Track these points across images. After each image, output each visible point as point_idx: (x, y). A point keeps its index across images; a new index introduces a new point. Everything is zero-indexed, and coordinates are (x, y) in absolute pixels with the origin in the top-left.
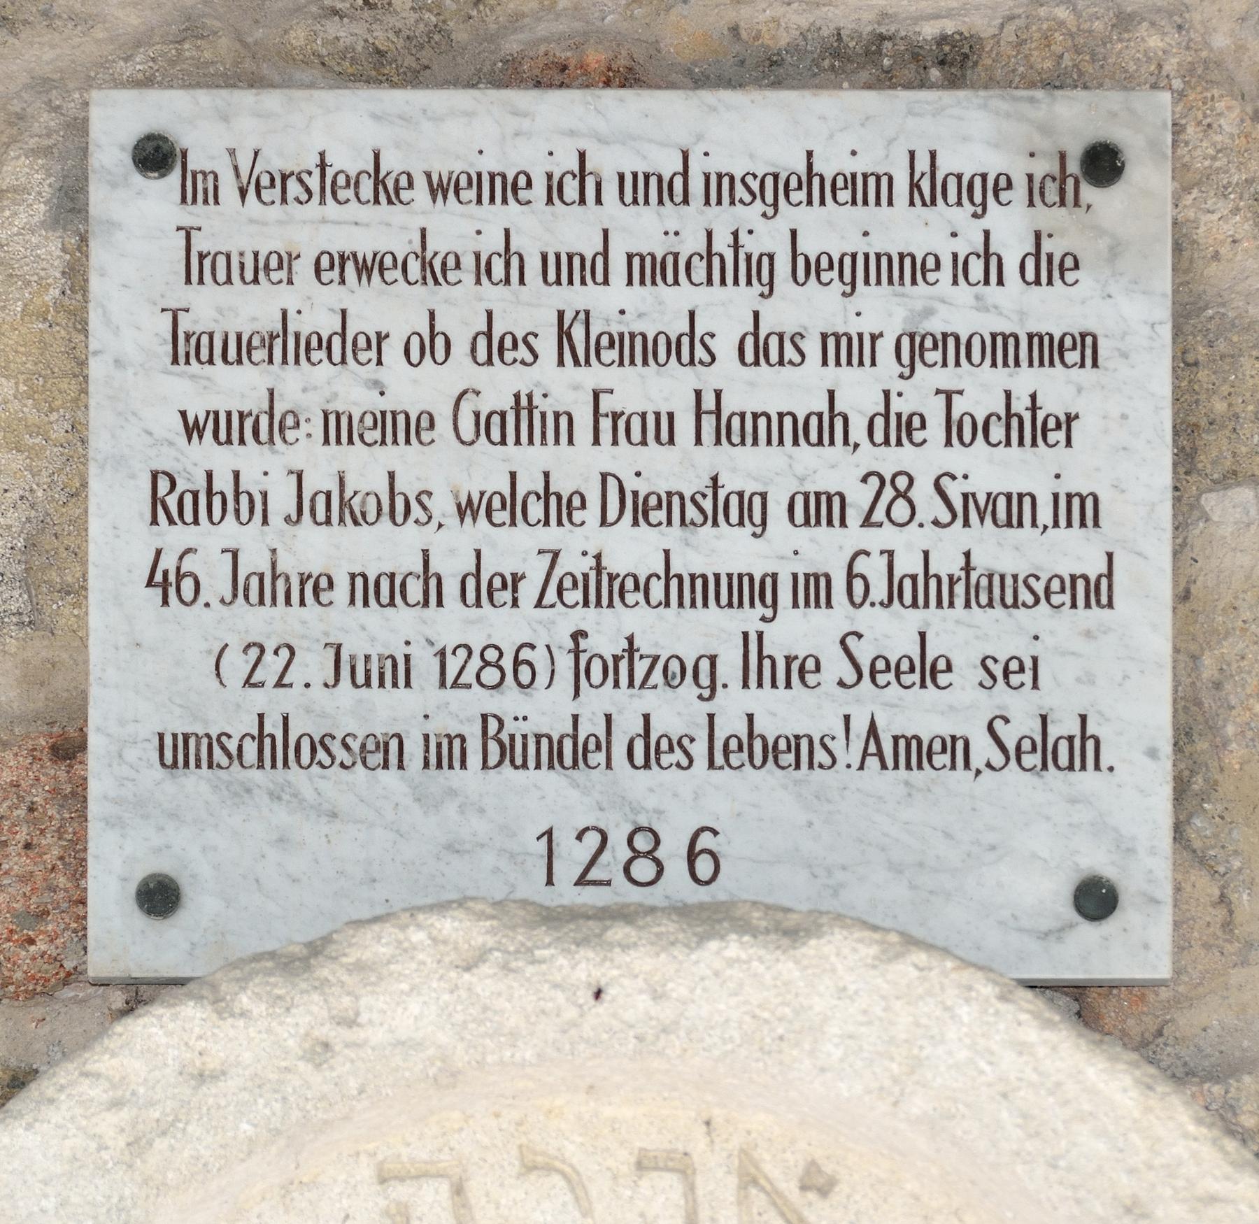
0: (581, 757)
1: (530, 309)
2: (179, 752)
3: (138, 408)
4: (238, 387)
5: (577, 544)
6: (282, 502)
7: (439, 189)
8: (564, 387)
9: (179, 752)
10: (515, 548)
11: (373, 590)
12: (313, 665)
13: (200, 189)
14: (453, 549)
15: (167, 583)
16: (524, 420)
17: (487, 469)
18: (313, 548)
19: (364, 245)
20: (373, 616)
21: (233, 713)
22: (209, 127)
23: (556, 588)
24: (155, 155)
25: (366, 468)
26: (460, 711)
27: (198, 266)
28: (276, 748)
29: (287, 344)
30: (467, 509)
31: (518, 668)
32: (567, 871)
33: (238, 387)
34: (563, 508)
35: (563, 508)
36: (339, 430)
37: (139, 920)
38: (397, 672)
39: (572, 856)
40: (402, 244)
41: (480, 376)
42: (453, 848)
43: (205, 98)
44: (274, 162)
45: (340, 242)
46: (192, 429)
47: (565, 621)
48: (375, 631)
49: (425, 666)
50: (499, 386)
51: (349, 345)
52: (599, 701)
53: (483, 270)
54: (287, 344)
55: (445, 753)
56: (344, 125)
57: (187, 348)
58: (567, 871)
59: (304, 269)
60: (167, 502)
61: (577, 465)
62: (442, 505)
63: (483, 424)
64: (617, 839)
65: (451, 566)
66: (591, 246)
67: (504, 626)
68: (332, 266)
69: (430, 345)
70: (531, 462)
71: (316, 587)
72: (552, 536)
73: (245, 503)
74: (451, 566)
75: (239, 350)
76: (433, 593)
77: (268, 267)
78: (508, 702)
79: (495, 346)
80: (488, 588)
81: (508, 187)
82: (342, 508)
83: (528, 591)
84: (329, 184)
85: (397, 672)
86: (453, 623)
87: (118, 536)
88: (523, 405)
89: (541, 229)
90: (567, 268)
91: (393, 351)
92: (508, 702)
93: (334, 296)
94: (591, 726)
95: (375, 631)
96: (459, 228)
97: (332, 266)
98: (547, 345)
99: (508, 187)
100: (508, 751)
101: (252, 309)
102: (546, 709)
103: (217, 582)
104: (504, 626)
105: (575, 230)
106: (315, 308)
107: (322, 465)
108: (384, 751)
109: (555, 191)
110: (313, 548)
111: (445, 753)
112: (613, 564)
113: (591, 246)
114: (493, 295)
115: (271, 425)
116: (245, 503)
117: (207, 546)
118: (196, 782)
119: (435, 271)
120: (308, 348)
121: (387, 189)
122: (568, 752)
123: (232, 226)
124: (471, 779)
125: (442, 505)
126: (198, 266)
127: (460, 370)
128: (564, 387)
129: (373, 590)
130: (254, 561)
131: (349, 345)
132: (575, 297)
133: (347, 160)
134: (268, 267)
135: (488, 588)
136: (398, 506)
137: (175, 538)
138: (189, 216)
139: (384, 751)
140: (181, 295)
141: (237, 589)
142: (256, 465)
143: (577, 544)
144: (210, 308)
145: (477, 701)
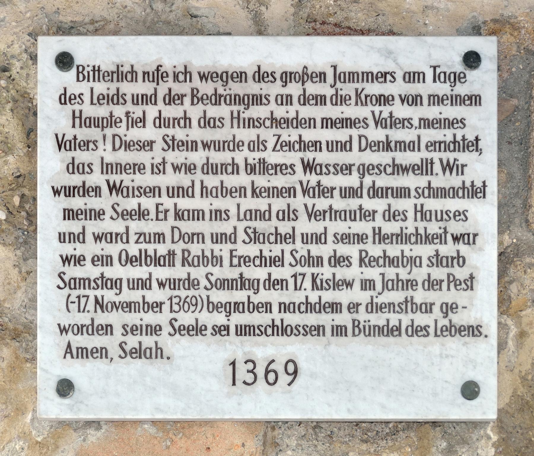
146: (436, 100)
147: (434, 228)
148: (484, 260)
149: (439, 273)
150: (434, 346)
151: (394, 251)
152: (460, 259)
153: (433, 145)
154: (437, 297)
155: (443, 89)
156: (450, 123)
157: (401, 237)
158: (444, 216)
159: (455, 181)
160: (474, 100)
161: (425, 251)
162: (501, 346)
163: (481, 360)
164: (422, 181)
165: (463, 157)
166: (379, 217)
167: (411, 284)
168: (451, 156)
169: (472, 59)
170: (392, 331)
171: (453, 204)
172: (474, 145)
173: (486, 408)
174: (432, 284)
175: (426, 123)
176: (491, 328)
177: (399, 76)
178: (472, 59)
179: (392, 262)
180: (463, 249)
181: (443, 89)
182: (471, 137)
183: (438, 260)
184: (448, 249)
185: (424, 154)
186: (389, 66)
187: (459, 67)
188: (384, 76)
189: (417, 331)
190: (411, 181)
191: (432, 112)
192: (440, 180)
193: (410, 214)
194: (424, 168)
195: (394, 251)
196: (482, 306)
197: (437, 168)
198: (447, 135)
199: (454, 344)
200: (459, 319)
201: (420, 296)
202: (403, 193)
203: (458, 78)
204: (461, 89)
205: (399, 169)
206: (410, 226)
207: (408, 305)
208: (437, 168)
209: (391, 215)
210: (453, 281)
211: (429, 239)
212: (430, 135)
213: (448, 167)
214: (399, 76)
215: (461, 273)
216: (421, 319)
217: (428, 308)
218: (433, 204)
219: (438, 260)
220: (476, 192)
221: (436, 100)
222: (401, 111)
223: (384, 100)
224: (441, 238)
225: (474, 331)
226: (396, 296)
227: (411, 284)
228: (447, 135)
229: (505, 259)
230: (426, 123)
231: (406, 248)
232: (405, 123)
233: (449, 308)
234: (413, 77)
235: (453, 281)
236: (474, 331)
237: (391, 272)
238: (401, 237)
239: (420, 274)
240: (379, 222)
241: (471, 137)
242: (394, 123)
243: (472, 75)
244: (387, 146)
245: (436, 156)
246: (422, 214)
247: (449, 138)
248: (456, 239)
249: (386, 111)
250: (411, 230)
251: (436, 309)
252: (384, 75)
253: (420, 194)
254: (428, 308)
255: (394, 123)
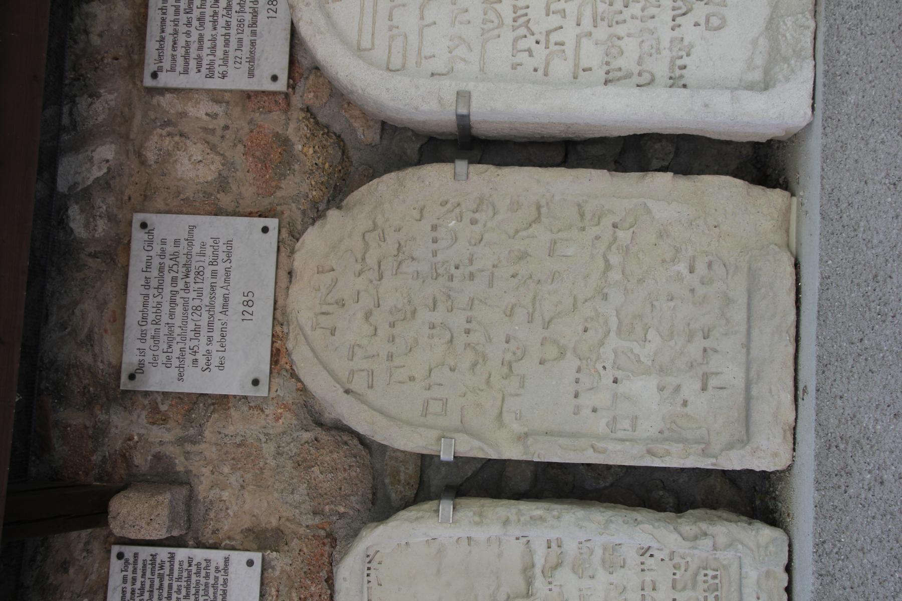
0: (256, 12)
1: (183, 18)
2: (251, 74)
3: (195, 80)
4: (193, 64)
5: (221, 12)
6: (212, 57)
7: (163, 32)
8: (196, 13)
9: (251, 74)
10: (222, 21)
11: (227, 43)
12: (238, 53)
13: (160, 69)
14: (221, 31)
15: (224, 76)
16: (201, 20)
17: (209, 25)
18: (220, 53)
19: (171, 43)
20: (231, 44)
21: (246, 66)
22: (150, 66)
23: (228, 15)
24: (154, 75)
25: (207, 44)
26: (247, 31)
27: (173, 70)
28: (251, 60)
29: (186, 58)
30: (215, 29)
31: (241, 22)
32: (274, 15)
33: (193, 64)
34: (216, 13)
35: (216, 13)
36: (200, 48)
37: (278, 82)
38: (240, 41)
39: (272, 14)
40: (171, 38)
41: (193, 26)
42: (269, 32)
43: (146, 68)
44: (157, 57)
45: (170, 48)
46: (199, 71)
47: (234, 14)
48: (233, 43)
49: (240, 36)
50: (195, 23)
51: (187, 45)
52: (247, 9)
53: (176, 25)
54: (186, 58)
55: (254, 33)
56: (152, 46)
57: (186, 71)
58: (274, 15)
59: (174, 53)
60: (210, 76)
61: (209, 11)
62: (214, 32)
63: (201, 26)
64: (269, 7)
65: (224, 31)
66: (174, 8)
67: (234, 23)
68: (174, 48)
69: (188, 34)
70: (208, 18)
71: (226, 52)
72: (220, 16)
73: (211, 64)
74: (224, 31)
75: (187, 63)
76: (228, 34)
77: (174, 58)
78: (246, 23)
79: (189, 24)
80: (228, 25)
81: (163, 20)
82: (213, 48)
83: (228, 19)
84: (161, 48)
85: (240, 41)
86: (233, 31)
87: (215, 84)
88: (199, 19)
89: (170, 16)
90: (177, 12)
91: (188, 40)
92: (246, 23)
93: (179, 49)
94: (251, 10)
95: (233, 43)
96: (169, 29)
97: (174, 48)
98: (189, 15)
99: (163, 20)
100: (254, 24)
101: (180, 61)
102: (248, 17)
103: (224, 68)
104: (234, 23)
105: (171, 11)
106: (181, 51)
107: (207, 51)
108: (253, 43)
109: (164, 14)
110: (220, 53)
111: (254, 33)
112: (225, 6)
113: (174, 8)
114: (181, 24)
115: (199, 59)
116: (211, 64)
117: (218, 69)
118: (256, 72)
119: (176, 33)
120: (187, 52)
121: (162, 39)
122: (255, 14)
123: (167, 63)
124: (258, 29)
125: (214, 32)
126: (173, 70)
127: (193, 29)
128: (196, 13)
129: (227, 43)
130: (221, 62)
131: (187, 45)
132: (182, 11)
133: (157, 46)
134: (174, 58)
135: (228, 25)
136: (214, 40)
137: (216, 74)
138: (165, 71)
139: (253, 43)
140: (177, 72)
141: (226, 65)
142: (205, 61)
143: (221, 12)
144: (180, 67)
145: (246, 28)
146: (135, 571)
147: (185, 574)
148: (200, 554)
149: (203, 573)
150: (232, 576)
151: (193, 591)
152: (199, 564)
153: (153, 573)
154: (213, 574)
155: (131, 568)
156: (144, 566)
157: (188, 588)
158: (181, 570)
159: (167, 565)
160: (136, 555)
161: (194, 578)
162: (233, 548)
163: (239, 558)
164: (166, 578)
165: (158, 561)
166: (179, 596)
167: (206, 584)
168: (157, 566)
169: (120, 556)
170: (225, 593)
171: (176, 566)
172: (154, 556)
173: (257, 557)
174: (207, 576)
175: (144, 575)
176: (226, 553)
177: (124, 585)
178: (120, 556)
179: (197, 592)
180: (194, 563)
181: (131, 568)
182: (151, 558)
183: (198, 573)
184: (194, 569)
185: (156, 577)
186: (120, 589)
187: (123, 561)
188: (124, 592)
189: (225, 582)
190: (166, 583)
191: (139, 572)
192: (167, 571)
193: (179, 583)
194: (161, 577)
195: (193, 591)
196: (217, 556)
197: (161, 572)
198: (149, 567)
199: (231, 569)
200: (221, 566)
201: (211, 581)
202: (170, 586)
203: (127, 561)
204: (131, 560)
205: (161, 587)
206: (184, 584)
207: (215, 586)
208: (161, 572)
209: (179, 591)
210: (207, 568)
211: (189, 577)
212: (148, 574)
213: (162, 568)
214: (124, 585)
215: (204, 564)
216: (221, 581)
217: (216, 578)
218: (176, 574)
219: (198, 573)
220: (172, 556)
221: (135, 571)
222: (138, 585)
223: (133, 591)
224: (189, 572)
225: (227, 560)
226: (211, 591)
227: (206, 584)
228: (149, 567)
229: (200, 545)
230: (144, 575)
231: (192, 586)
232: (143, 584)
233: (217, 570)
234: (125, 580)
235: (207, 568)
236: (227, 560)
237: (202, 593)
238: (188, 588)
239: (203, 581)
240: (181, 596)
241: (151, 558)
242: (142, 588)
243: (126, 556)
244: (151, 591)
245: (157, 572)
246: (179, 579)
247: (150, 566)
248: (190, 566)
249: (137, 591)
250: (185, 583)
251: (217, 575)
252: (123, 591)
253: (171, 579)
254: (216, 578)
255: (142, 588)
